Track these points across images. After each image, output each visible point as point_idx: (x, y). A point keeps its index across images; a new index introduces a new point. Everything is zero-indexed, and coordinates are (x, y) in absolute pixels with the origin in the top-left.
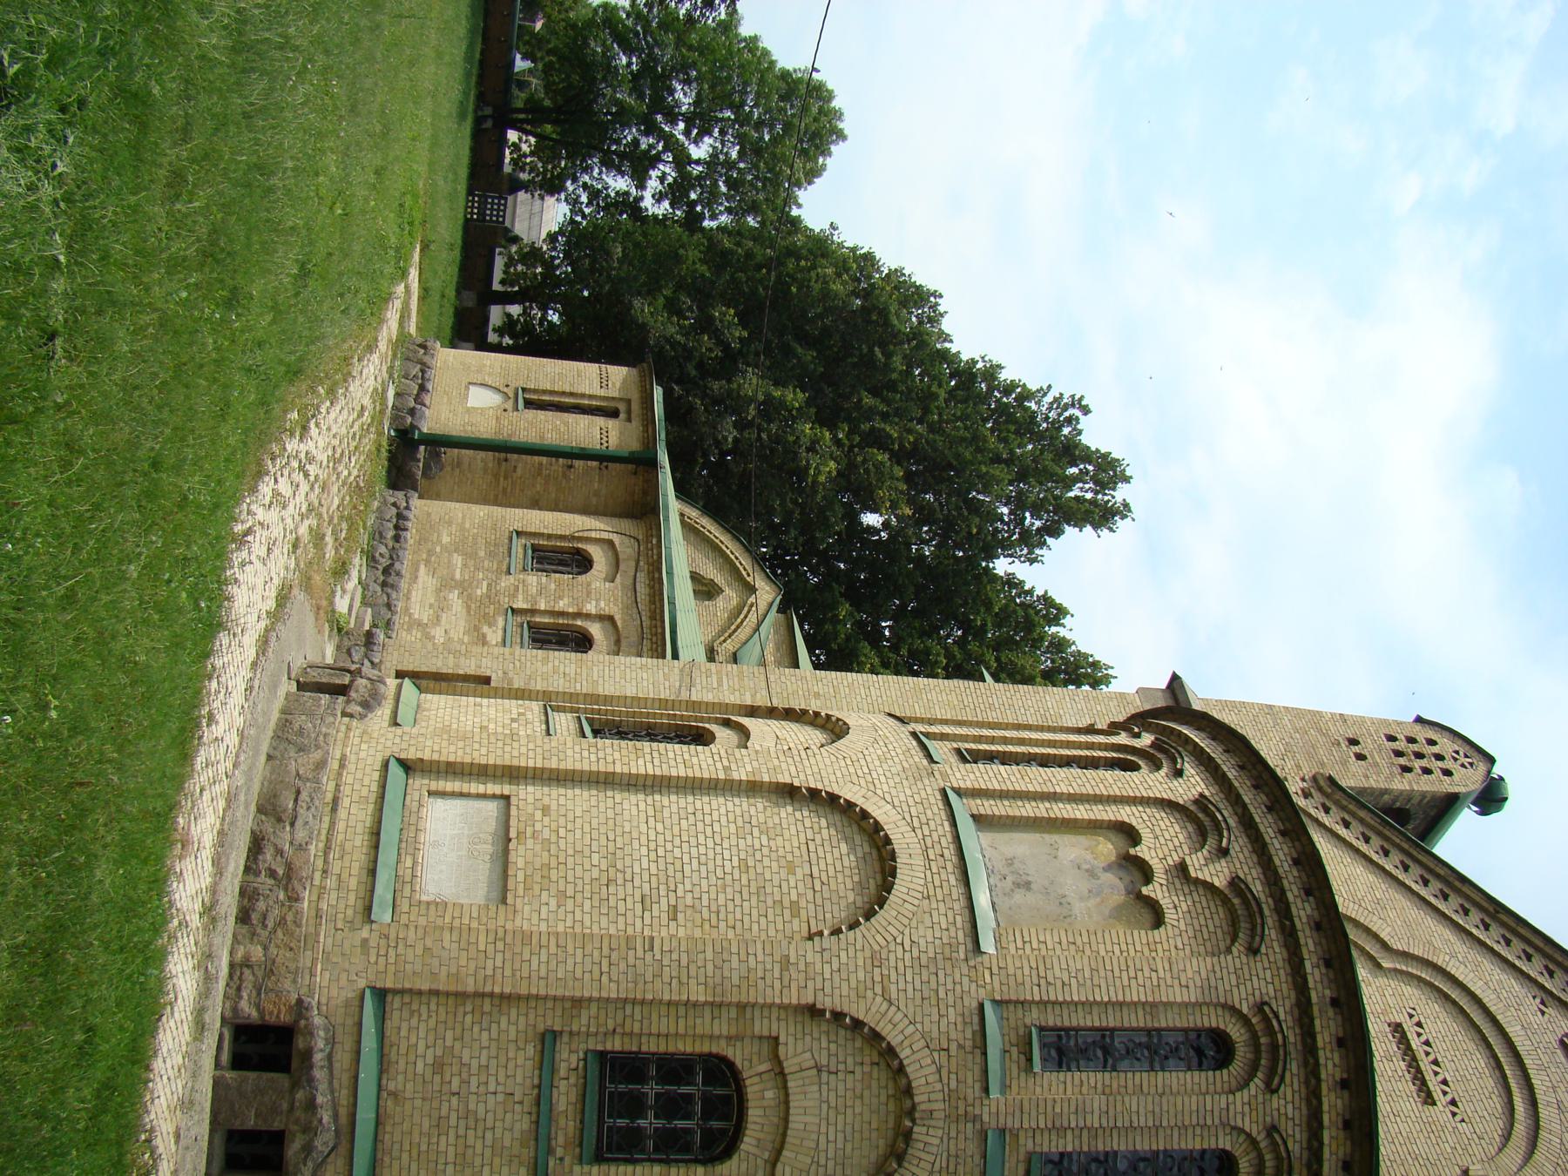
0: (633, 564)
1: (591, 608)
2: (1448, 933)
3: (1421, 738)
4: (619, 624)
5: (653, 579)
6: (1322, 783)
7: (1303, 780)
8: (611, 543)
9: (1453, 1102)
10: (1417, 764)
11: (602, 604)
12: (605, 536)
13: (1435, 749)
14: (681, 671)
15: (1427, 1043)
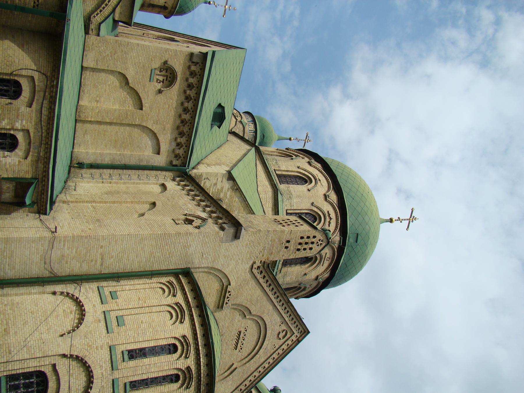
0: (42, 94)
1: (18, 125)
2: (271, 308)
3: (308, 250)
4: (32, 135)
5: (50, 108)
6: (265, 265)
7: (261, 261)
8: (32, 78)
9: (241, 349)
10: (307, 240)
11: (24, 122)
12: (30, 73)
13: (314, 240)
14: (49, 241)
15: (245, 335)
